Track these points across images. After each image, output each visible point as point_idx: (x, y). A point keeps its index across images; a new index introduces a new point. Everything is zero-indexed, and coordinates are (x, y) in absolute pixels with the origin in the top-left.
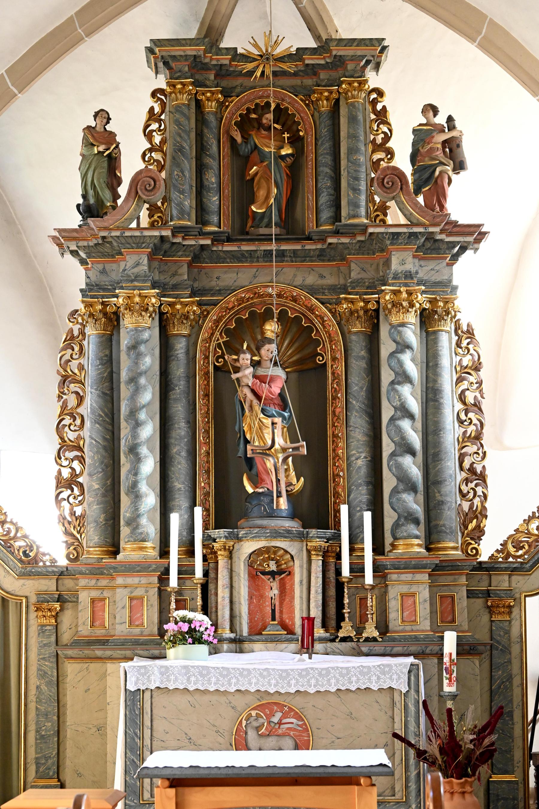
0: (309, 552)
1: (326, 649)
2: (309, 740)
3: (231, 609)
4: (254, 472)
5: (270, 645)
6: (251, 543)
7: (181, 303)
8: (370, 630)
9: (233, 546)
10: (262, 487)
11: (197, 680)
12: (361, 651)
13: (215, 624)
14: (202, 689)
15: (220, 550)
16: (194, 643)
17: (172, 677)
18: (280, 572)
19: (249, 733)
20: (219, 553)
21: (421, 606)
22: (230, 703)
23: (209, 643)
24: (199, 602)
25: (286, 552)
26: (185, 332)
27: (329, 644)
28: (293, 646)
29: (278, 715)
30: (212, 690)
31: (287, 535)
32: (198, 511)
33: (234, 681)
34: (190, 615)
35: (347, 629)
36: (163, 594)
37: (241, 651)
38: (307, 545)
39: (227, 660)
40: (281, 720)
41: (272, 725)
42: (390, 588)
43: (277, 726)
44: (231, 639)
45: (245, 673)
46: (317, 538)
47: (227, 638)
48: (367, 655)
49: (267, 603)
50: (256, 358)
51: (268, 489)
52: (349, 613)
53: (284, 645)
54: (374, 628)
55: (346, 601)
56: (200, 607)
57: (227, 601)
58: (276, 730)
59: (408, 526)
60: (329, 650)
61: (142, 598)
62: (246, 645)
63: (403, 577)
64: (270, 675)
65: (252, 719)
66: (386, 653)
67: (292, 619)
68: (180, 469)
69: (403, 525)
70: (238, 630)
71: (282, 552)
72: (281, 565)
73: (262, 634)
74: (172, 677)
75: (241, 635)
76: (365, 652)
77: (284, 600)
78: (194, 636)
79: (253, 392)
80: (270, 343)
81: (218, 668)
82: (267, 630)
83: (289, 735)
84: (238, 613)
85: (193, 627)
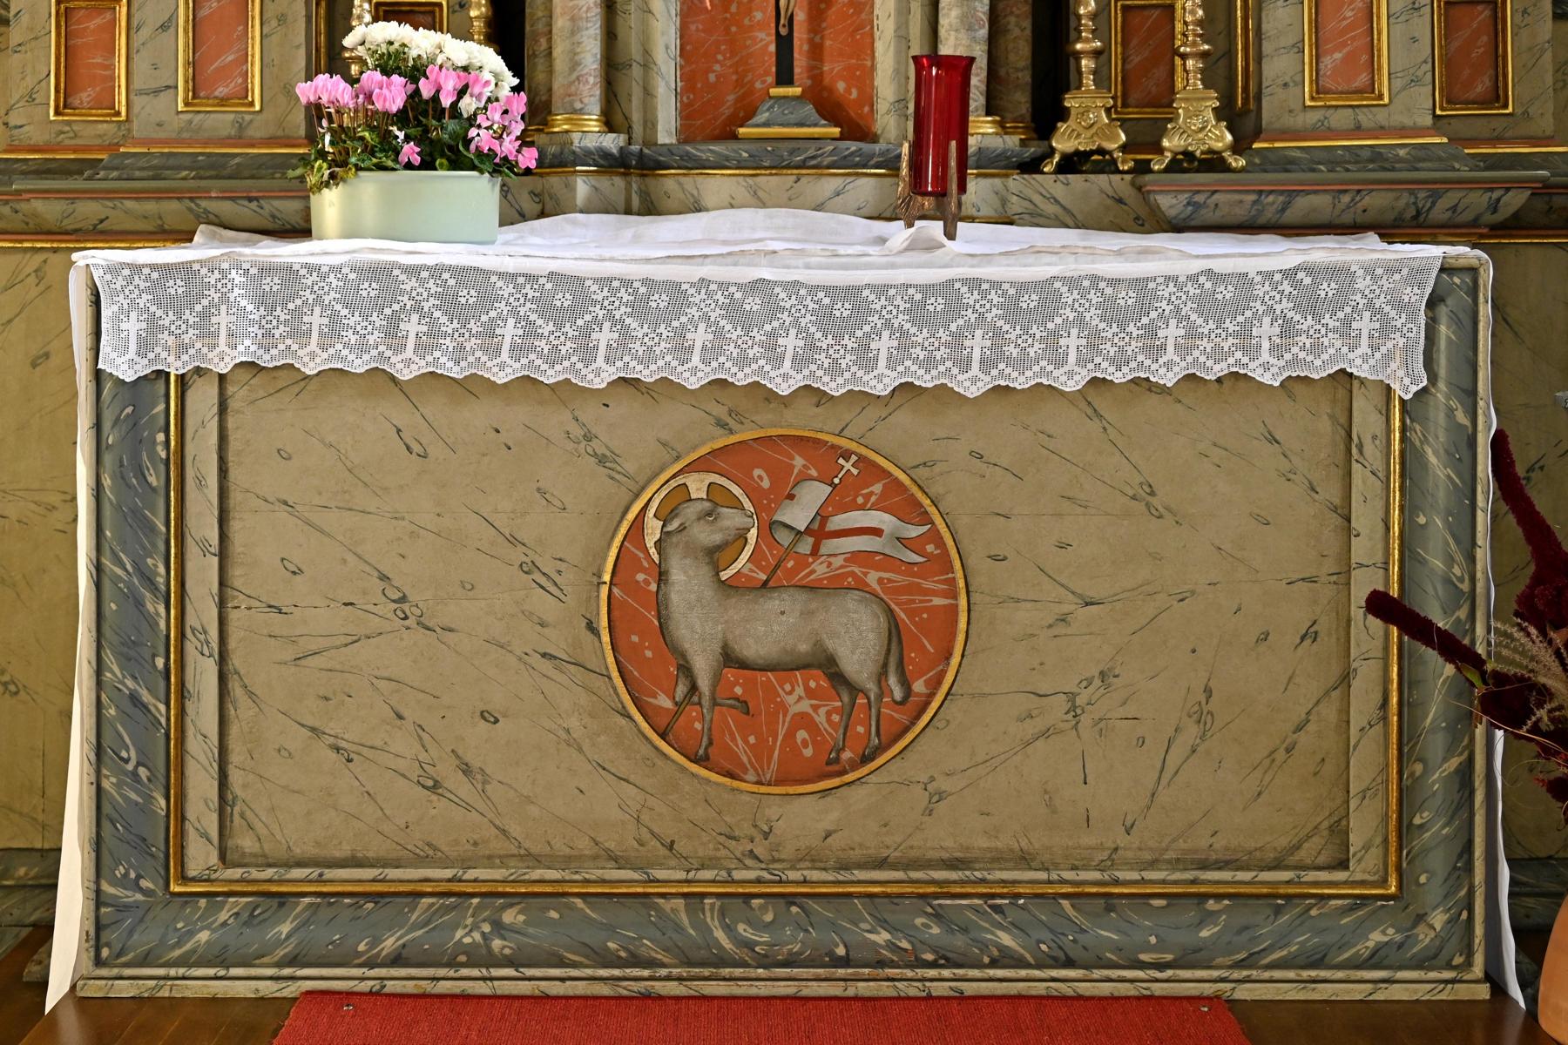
1: (1004, 202)
2: (953, 610)
3: (610, 36)
5: (770, 182)
8: (1196, 123)
11: (434, 333)
12: (1155, 210)
14: (456, 373)
16: (427, 165)
17: (316, 320)
19: (677, 575)
21: (1398, 29)
22: (588, 437)
23: (498, 166)
27: (1017, 182)
28: (866, 187)
29: (813, 495)
30: (501, 378)
33: (604, 337)
35: (1088, 120)
37: (650, 208)
39: (582, 245)
40: (822, 516)
41: (784, 538)
43: (805, 546)
44: (605, 154)
45: (660, 301)
48: (1178, 227)
49: (758, 16)
52: (1097, 54)
53: (829, 185)
54: (1210, 115)
56: (478, 25)
58: (802, 563)
60: (1016, 205)
62: (671, 183)
64: (774, 310)
65: (691, 511)
66: (1262, 221)
67: (864, 76)
70: (636, 117)
73: (735, 137)
74: (316, 320)
75: (650, 142)
76: (1172, 213)
78: (431, 134)
81: (531, 278)
82: (757, 120)
83: (861, 586)
84: (635, 52)
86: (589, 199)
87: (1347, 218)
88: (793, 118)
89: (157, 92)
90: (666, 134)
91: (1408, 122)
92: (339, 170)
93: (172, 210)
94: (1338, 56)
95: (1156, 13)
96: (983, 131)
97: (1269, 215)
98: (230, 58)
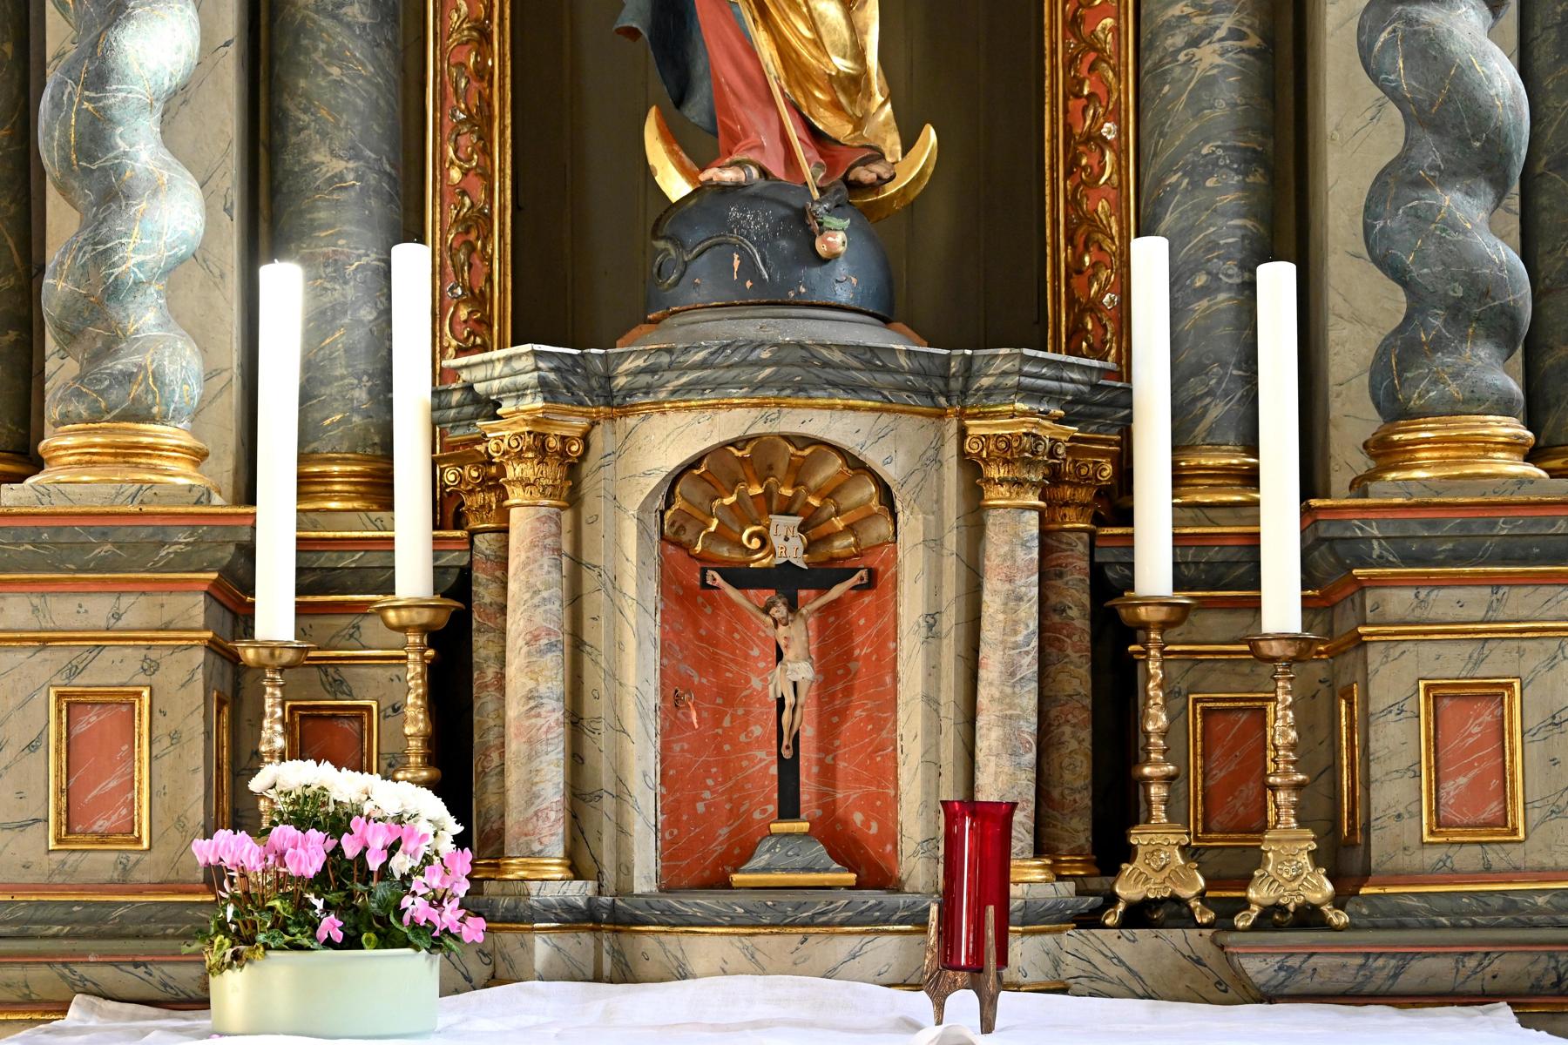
0: (971, 467)
1: (1056, 963)
3: (576, 758)
4: (695, 111)
5: (770, 943)
6: (675, 419)
8: (1288, 871)
9: (585, 438)
10: (739, 164)
12: (1240, 976)
13: (482, 838)
15: (520, 457)
16: (351, 942)
18: (824, 574)
20: (513, 471)
21: (1534, 749)
24: (415, 722)
25: (857, 466)
27: (1072, 939)
28: (887, 948)
31: (863, 377)
32: (413, 266)
34: (343, 785)
35: (1159, 862)
36: (234, 685)
37: (625, 974)
38: (963, 433)
42: (1374, 655)
44: (570, 908)
46: (1015, 391)
47: (548, 907)
49: (757, 731)
51: (764, 173)
52: (1169, 779)
53: (844, 945)
54: (1305, 860)
55: (1156, 720)
56: (414, 744)
57: (553, 715)
59: (1467, 350)
60: (1071, 967)
61: (124, 701)
62: (650, 944)
63: (1444, 602)
66: (1369, 988)
67: (885, 806)
68: (338, 84)
69: (1438, 344)
70: (608, 860)
71: (833, 467)
72: (828, 538)
73: (727, 885)
75: (624, 891)
76: (1260, 979)
77: (843, 713)
78: (357, 904)
82: (755, 863)
84: (606, 781)
85: (350, 851)
86: (550, 963)
87: (1474, 985)
88: (799, 861)
89: (22, 826)
90: (644, 879)
91: (1549, 862)
92: (244, 941)
93: (41, 978)
94: (1462, 780)
95: (1244, 717)
96: (1030, 879)
97: (1378, 982)
98: (113, 784)
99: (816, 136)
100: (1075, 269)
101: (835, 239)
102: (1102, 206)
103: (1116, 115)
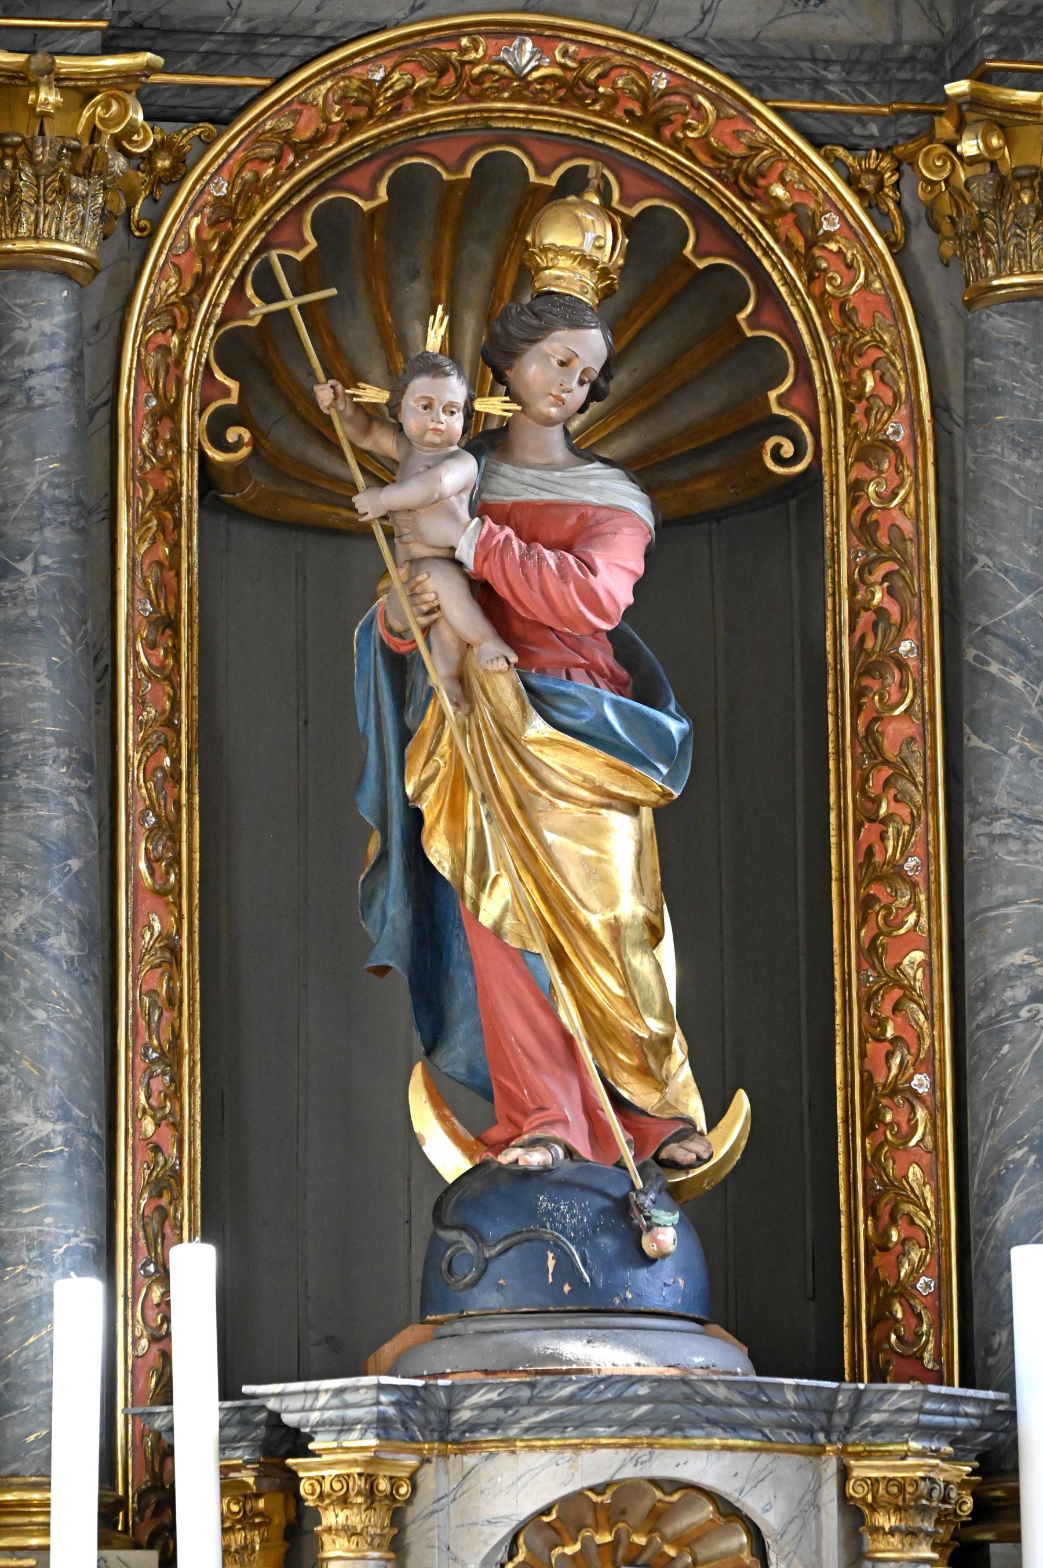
0: (854, 1516)
7: (60, 81)
15: (344, 1501)
20: (331, 1517)
25: (730, 1512)
26: (74, 246)
31: (746, 1414)
38: (844, 1473)
50: (494, 406)
51: (570, 1152)
68: (43, 1029)
79: (484, 594)
80: (576, 325)
99: (619, 1103)
100: (879, 1245)
101: (666, 1234)
102: (915, 1173)
103: (929, 1064)
